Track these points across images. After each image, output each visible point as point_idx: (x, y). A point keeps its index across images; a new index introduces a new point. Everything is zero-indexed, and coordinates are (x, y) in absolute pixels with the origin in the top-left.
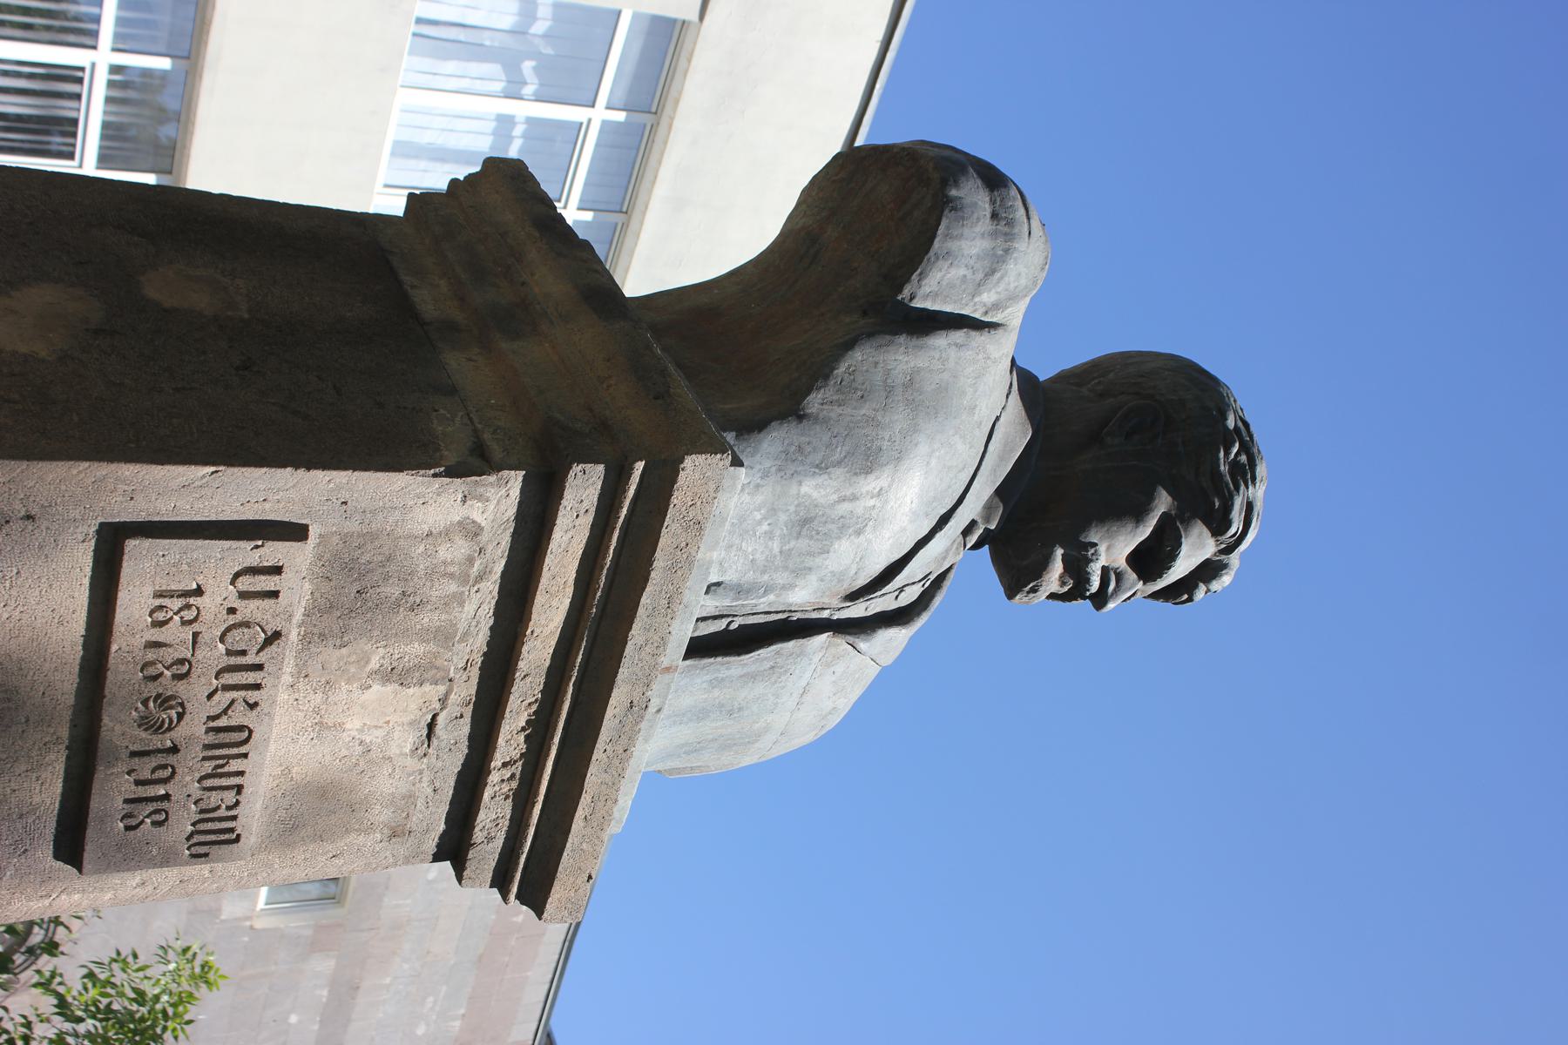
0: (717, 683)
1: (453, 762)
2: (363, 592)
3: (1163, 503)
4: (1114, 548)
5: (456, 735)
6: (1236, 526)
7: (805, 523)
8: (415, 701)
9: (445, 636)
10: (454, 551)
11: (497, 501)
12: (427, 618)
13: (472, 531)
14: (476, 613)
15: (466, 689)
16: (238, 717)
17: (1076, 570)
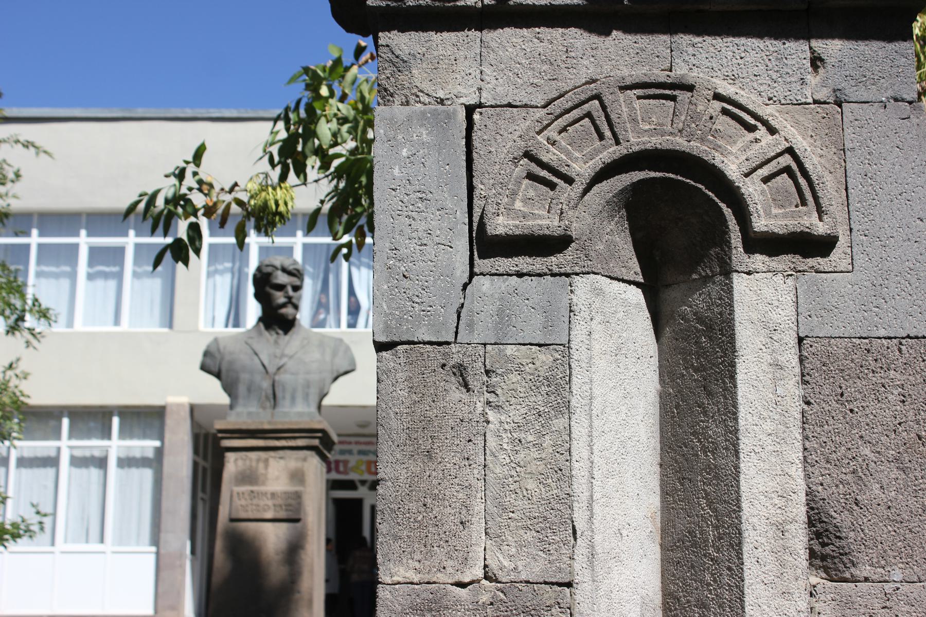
0: (284, 398)
1: (288, 452)
2: (248, 478)
3: (268, 289)
4: (280, 297)
5: (281, 453)
6: (269, 269)
7: (249, 390)
8: (272, 462)
9: (258, 460)
10: (240, 463)
11: (230, 457)
12: (254, 464)
13: (236, 460)
14: (253, 455)
15: (272, 453)
16: (269, 496)
17: (284, 305)
